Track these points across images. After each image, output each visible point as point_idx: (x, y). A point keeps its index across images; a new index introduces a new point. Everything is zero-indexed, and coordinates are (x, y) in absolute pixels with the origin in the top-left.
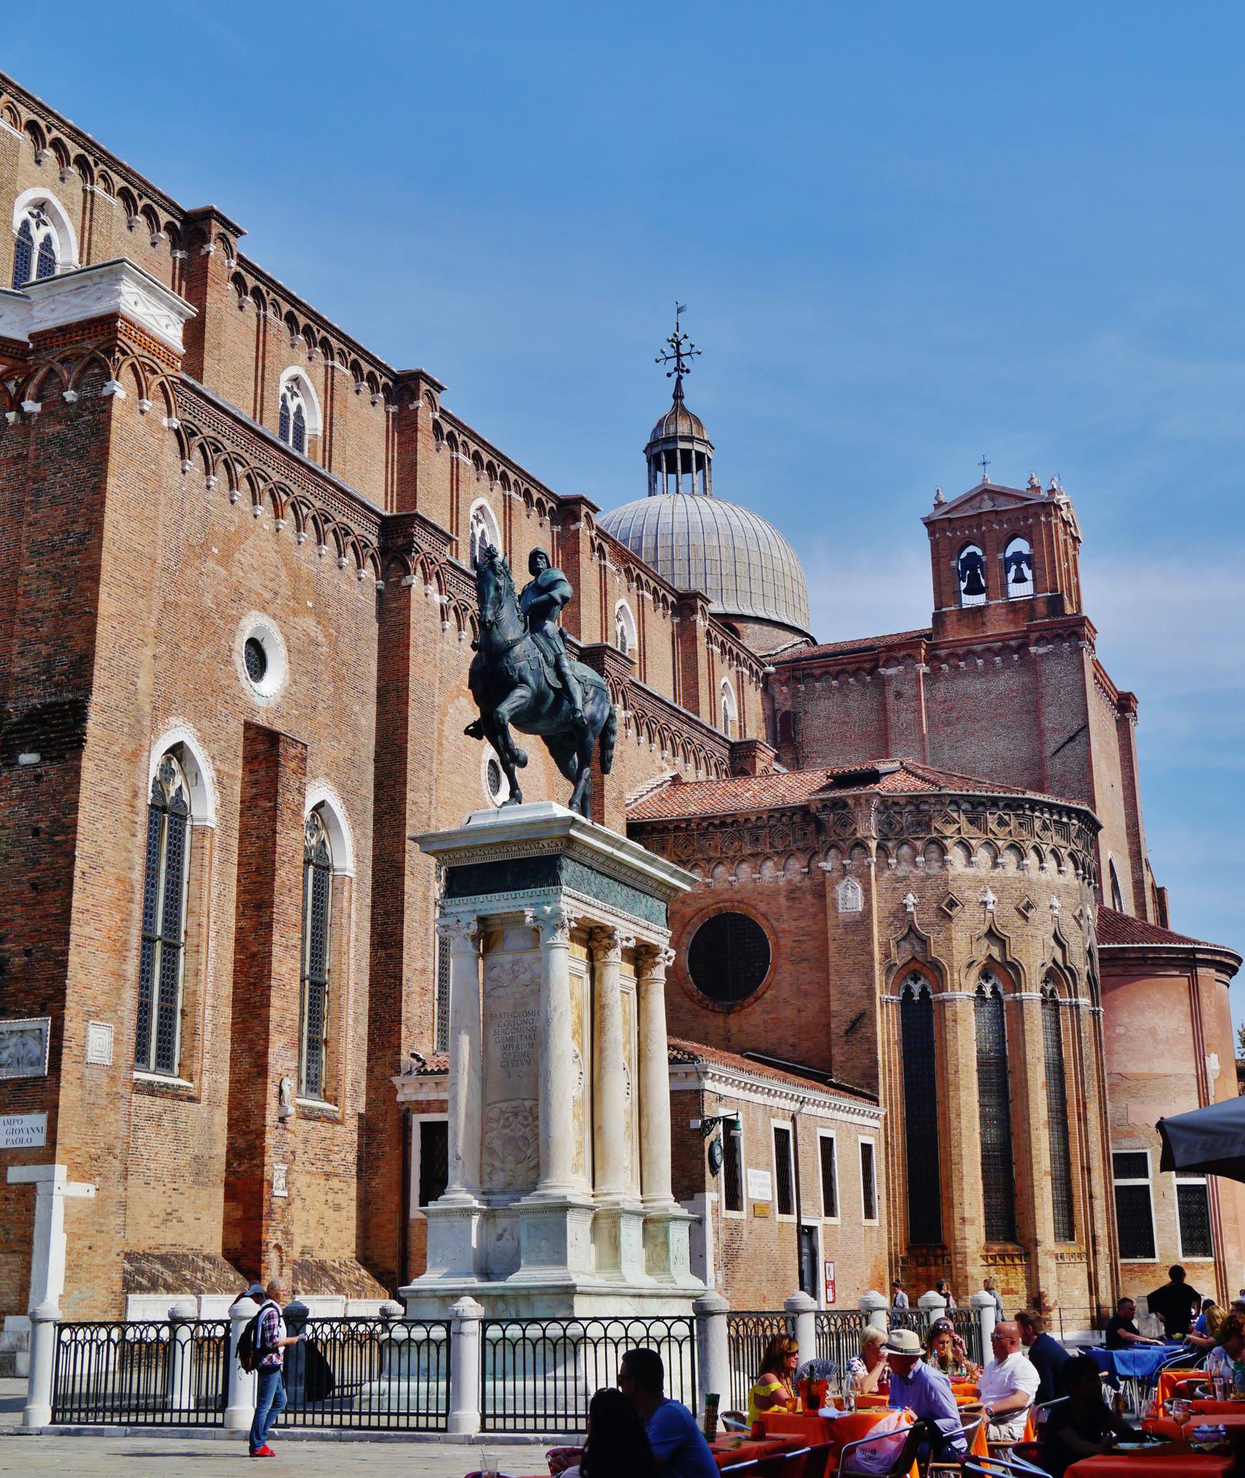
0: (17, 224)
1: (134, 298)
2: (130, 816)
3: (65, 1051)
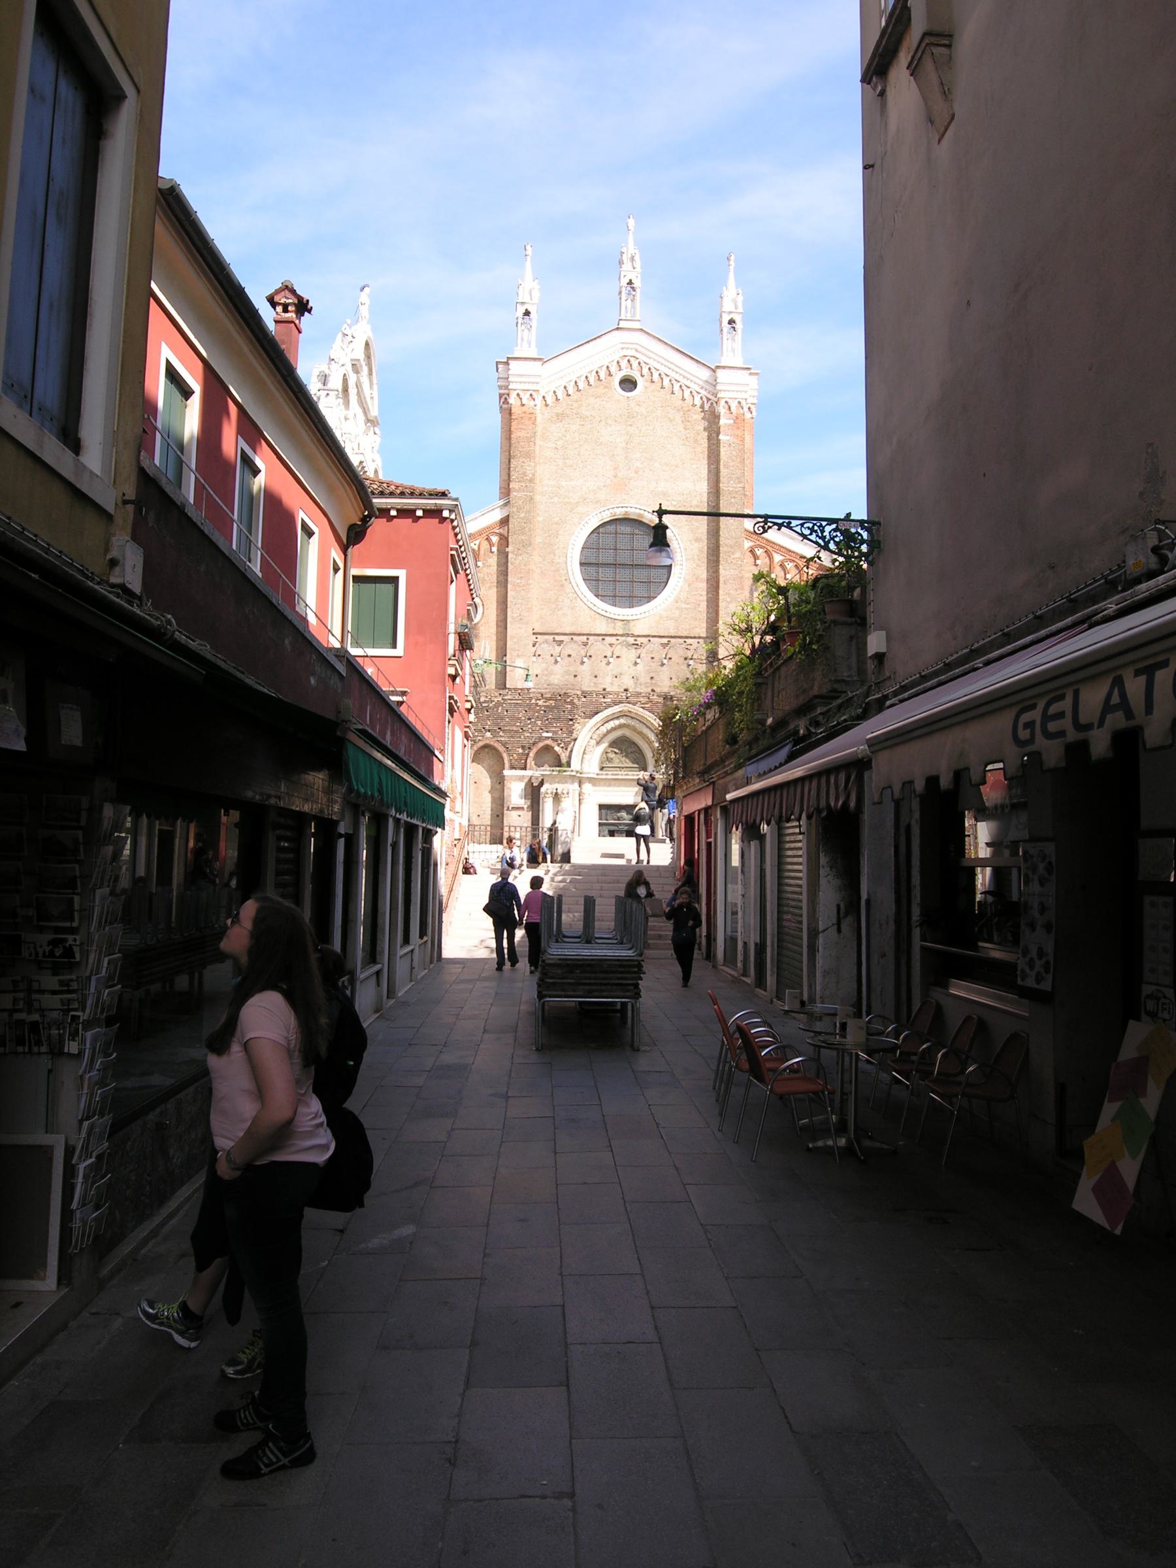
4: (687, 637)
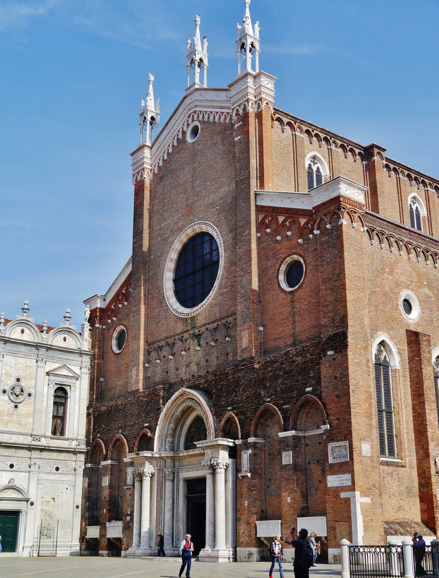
0: (307, 166)
1: (345, 189)
2: (367, 369)
3: (354, 452)
4: (227, 317)
